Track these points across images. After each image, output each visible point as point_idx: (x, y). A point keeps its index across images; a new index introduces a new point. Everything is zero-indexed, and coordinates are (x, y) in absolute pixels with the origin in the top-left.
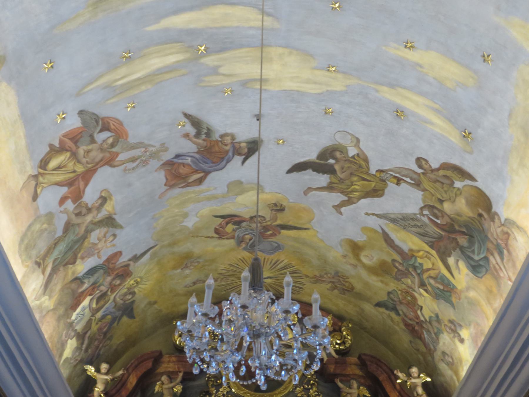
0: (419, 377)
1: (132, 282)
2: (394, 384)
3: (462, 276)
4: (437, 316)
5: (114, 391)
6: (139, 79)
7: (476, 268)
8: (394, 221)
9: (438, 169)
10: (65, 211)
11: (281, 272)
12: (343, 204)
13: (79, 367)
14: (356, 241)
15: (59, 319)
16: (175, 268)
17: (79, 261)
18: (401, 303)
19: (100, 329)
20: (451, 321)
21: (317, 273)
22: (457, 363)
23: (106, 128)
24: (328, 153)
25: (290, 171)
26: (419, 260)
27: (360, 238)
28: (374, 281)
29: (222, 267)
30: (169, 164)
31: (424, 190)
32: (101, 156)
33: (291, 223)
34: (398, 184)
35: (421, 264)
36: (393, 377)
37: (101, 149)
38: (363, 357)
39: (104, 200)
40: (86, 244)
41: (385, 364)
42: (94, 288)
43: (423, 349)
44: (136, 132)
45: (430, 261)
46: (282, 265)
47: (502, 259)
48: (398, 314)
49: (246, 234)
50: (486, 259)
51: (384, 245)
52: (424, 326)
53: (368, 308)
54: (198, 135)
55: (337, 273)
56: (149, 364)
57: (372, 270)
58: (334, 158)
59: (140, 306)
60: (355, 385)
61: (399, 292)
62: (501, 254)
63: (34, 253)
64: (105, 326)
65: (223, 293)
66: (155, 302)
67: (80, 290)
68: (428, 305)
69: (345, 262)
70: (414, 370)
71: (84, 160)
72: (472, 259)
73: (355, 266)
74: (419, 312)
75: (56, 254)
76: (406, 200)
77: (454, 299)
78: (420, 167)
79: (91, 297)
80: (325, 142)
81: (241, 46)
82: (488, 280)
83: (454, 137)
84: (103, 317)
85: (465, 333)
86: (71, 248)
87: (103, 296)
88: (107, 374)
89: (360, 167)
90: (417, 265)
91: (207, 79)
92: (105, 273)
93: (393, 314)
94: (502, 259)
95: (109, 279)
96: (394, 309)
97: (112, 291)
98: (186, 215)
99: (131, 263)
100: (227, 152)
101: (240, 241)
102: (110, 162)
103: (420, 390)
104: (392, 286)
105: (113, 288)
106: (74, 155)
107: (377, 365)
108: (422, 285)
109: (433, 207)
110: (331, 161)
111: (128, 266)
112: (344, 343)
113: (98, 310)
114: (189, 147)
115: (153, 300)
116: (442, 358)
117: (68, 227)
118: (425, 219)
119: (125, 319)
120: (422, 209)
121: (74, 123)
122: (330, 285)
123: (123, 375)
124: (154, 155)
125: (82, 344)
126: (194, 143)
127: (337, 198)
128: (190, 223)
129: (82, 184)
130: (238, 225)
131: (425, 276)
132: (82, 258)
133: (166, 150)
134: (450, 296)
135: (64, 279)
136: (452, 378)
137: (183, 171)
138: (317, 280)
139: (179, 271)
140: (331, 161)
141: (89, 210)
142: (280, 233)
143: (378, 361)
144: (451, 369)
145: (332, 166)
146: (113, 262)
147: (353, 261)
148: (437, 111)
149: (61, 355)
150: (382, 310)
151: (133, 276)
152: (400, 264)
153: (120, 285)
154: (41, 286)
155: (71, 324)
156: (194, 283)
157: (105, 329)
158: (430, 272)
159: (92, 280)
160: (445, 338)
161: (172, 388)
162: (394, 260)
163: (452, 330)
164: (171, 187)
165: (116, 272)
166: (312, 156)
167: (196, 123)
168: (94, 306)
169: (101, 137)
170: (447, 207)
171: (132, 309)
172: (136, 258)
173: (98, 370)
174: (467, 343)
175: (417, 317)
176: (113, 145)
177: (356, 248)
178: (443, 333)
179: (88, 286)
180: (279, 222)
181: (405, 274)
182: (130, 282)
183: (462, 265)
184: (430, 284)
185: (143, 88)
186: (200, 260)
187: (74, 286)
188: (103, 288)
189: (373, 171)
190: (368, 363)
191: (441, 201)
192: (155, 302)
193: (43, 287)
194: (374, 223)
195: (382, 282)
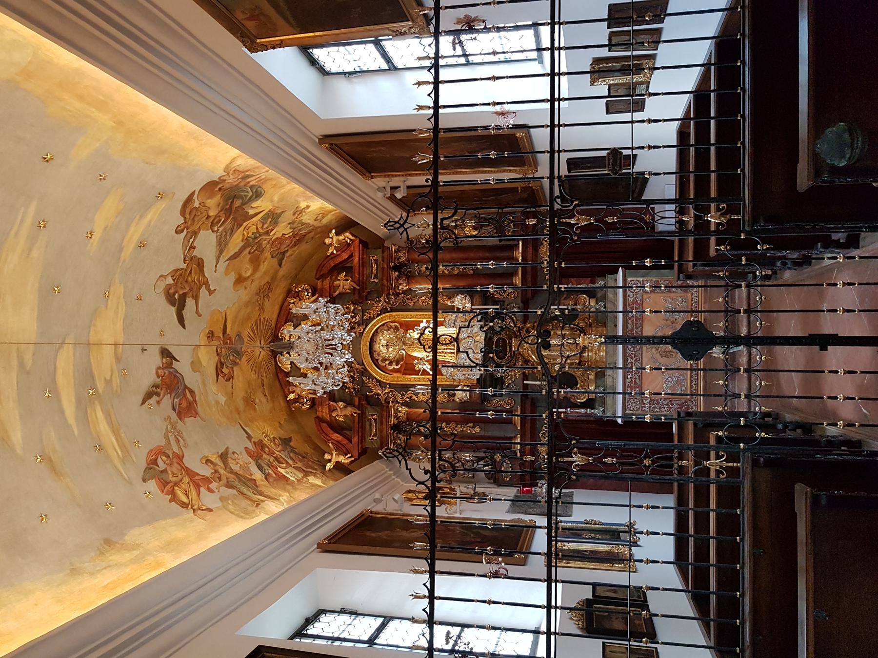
2: (337, 255)
3: (262, 205)
4: (289, 224)
6: (117, 439)
7: (258, 195)
8: (221, 252)
9: (185, 218)
10: (218, 488)
12: (208, 288)
15: (296, 489)
16: (255, 409)
17: (253, 477)
19: (300, 461)
20: (294, 214)
21: (257, 308)
23: (155, 462)
24: (170, 298)
25: (184, 327)
26: (250, 235)
27: (233, 276)
28: (263, 267)
30: (180, 415)
31: (199, 229)
32: (176, 465)
34: (194, 248)
37: (171, 464)
39: (208, 461)
40: (241, 472)
44: (158, 440)
45: (251, 227)
47: (253, 176)
50: (251, 187)
51: (238, 259)
53: (282, 272)
54: (158, 394)
55: (257, 294)
57: (256, 269)
58: (174, 294)
60: (338, 282)
62: (249, 176)
63: (250, 509)
68: (282, 229)
70: (327, 241)
71: (180, 477)
72: (251, 197)
73: (253, 280)
75: (249, 493)
76: (206, 243)
77: (279, 211)
78: (182, 231)
80: (163, 300)
81: (89, 362)
82: (266, 187)
83: (162, 205)
84: (292, 459)
85: (303, 205)
87: (276, 459)
88: (332, 455)
89: (181, 275)
91: (115, 389)
93: (287, 254)
94: (253, 176)
95: (265, 456)
96: (284, 253)
98: (217, 402)
100: (170, 372)
101: (235, 363)
102: (180, 458)
103: (341, 238)
104: (267, 254)
105: (271, 453)
106: (176, 484)
108: (267, 233)
109: (212, 223)
110: (176, 296)
112: (307, 290)
113: (287, 463)
114: (167, 401)
115: (278, 425)
117: (229, 486)
118: (221, 229)
119: (292, 444)
120: (213, 231)
121: (152, 485)
123: (332, 443)
124: (174, 427)
126: (164, 397)
127: (203, 291)
128: (223, 399)
129: (197, 477)
131: (261, 231)
132: (251, 475)
133: (169, 417)
137: (184, 404)
138: (262, 308)
140: (176, 296)
141: (216, 471)
143: (320, 267)
145: (180, 296)
147: (249, 282)
148: (141, 217)
149: (321, 486)
150: (284, 262)
156: (265, 395)
159: (266, 467)
160: (306, 218)
164: (197, 413)
166: (173, 310)
167: (148, 396)
169: (162, 465)
170: (212, 213)
172: (249, 437)
173: (330, 461)
174: (310, 203)
175: (290, 237)
176: (168, 456)
177: (240, 280)
180: (221, 335)
181: (259, 244)
182: (266, 441)
183: (254, 205)
185: (123, 435)
187: (271, 480)
188: (272, 459)
189: (184, 266)
191: (208, 217)
194: (222, 265)
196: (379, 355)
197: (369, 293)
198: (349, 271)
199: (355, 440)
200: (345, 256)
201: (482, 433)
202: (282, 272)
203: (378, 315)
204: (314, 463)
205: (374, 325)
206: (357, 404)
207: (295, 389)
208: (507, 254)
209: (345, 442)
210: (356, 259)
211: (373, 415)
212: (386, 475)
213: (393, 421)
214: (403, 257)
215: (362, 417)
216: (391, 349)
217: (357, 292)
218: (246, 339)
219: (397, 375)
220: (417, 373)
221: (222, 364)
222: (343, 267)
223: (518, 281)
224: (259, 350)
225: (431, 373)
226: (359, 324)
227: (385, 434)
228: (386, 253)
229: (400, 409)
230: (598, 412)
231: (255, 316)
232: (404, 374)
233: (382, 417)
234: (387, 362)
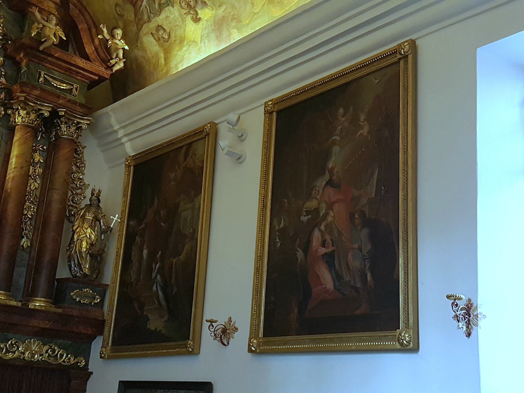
22: (175, 41)
36: (94, 30)
41: (90, 14)
70: (119, 32)
107: (80, 10)
116: (154, 32)
136: (157, 54)
144: (161, 46)
163: (189, 5)
178: (173, 6)
198: (62, 45)
200: (89, 49)
210: (81, 62)
222: (73, 39)
228: (79, 109)
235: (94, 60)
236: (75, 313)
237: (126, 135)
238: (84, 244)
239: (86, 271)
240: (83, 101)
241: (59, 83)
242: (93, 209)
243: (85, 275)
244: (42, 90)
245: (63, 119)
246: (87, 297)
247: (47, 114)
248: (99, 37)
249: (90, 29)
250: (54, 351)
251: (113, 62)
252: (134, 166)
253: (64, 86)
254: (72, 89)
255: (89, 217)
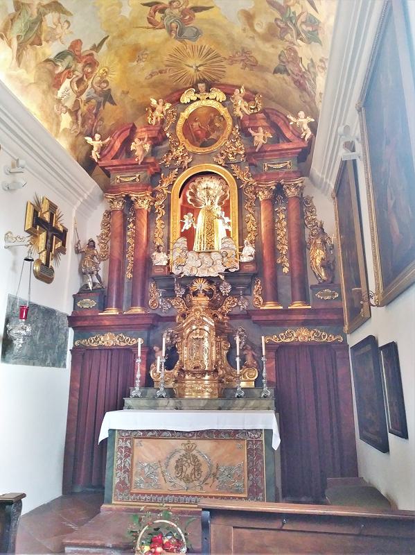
0: (305, 118)
1: (101, 71)
2: (288, 126)
5: (106, 152)
11: (208, 57)
13: (80, 138)
14: (247, 9)
16: (131, 60)
18: (288, 62)
19: (89, 110)
28: (266, 47)
29: (165, 58)
33: (200, 4)
35: (294, 13)
36: (287, 122)
38: (267, 111)
42: (69, 72)
43: (308, 99)
46: (205, 51)
48: (289, 75)
49: (171, 23)
52: (306, 76)
56: (128, 133)
59: (117, 94)
61: (285, 51)
64: (93, 109)
65: (174, 84)
66: (128, 92)
67: (57, 72)
69: (247, 36)
70: (301, 114)
74: (300, 65)
79: (70, 80)
84: (88, 100)
86: (30, 29)
87: (80, 82)
90: (292, 15)
92: (74, 59)
93: (285, 76)
96: (286, 71)
97: (89, 80)
99: (94, 52)
101: (170, 31)
103: (305, 126)
105: (88, 75)
111: (92, 55)
115: (125, 89)
119: (108, 104)
122: (241, 64)
123: (110, 141)
125: (77, 119)
130: (163, 13)
131: (298, 24)
134: (318, 34)
135: (36, 58)
138: (232, 61)
139: (136, 63)
142: (194, 16)
143: (277, 113)
146: (76, 49)
147: (251, 34)
150: (278, 75)
151: (100, 65)
152: (281, 21)
153: (92, 72)
154: (13, 59)
155: (59, 101)
156: (151, 75)
157: (94, 111)
158: (301, 17)
161: (142, 145)
162: (276, 20)
165: (84, 60)
168: (76, 89)
171: (111, 97)
172: (96, 48)
173: (94, 139)
175: (300, 71)
177: (249, 17)
179: (63, 69)
180: (190, 5)
181: (285, 30)
182: (99, 71)
184: (303, 31)
186: (148, 52)
187: (49, 66)
190: (270, 115)
192: (128, 92)
193: (15, 60)
195: (273, 46)
196: (199, 182)
197: (256, 166)
199: (115, 162)
200: (288, 135)
201: (126, 281)
202: (270, 77)
203: (235, 177)
204: (86, 120)
205: (225, 174)
206: (148, 161)
207: (161, 104)
208: (298, 295)
209: (113, 153)
210: (285, 146)
211: (139, 177)
212: (81, 192)
213: (133, 196)
214: (291, 192)
215: (135, 167)
216: (203, 192)
217: (253, 150)
218: (197, 43)
219: (180, 201)
220: (182, 218)
221: (162, 11)
222: (279, 136)
223: (270, 306)
224: (193, 66)
225: (182, 231)
226: (227, 159)
227: (122, 189)
228: (293, 175)
229: (145, 202)
230: (136, 391)
231: (225, 53)
232: (182, 207)
233: (137, 185)
234: (192, 190)
235: (294, 140)
236: (322, 306)
237: (327, 178)
238: (317, 261)
239: (325, 278)
240: (296, 169)
241: (277, 165)
242: (321, 236)
243: (324, 281)
244: (266, 174)
245: (284, 186)
246: (328, 294)
247: (274, 188)
248: (291, 123)
249: (285, 122)
250: (318, 334)
251: (304, 134)
252: (337, 196)
253: (281, 166)
254: (286, 166)
255: (319, 242)
